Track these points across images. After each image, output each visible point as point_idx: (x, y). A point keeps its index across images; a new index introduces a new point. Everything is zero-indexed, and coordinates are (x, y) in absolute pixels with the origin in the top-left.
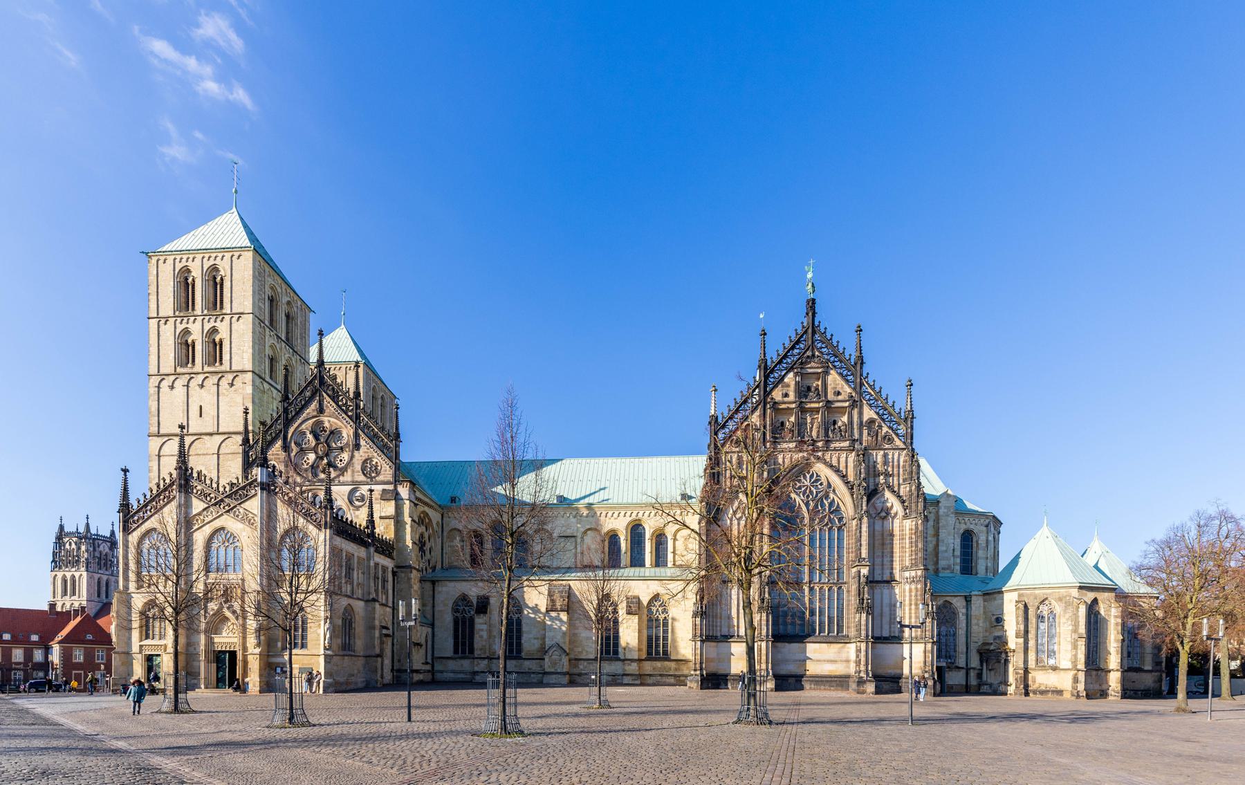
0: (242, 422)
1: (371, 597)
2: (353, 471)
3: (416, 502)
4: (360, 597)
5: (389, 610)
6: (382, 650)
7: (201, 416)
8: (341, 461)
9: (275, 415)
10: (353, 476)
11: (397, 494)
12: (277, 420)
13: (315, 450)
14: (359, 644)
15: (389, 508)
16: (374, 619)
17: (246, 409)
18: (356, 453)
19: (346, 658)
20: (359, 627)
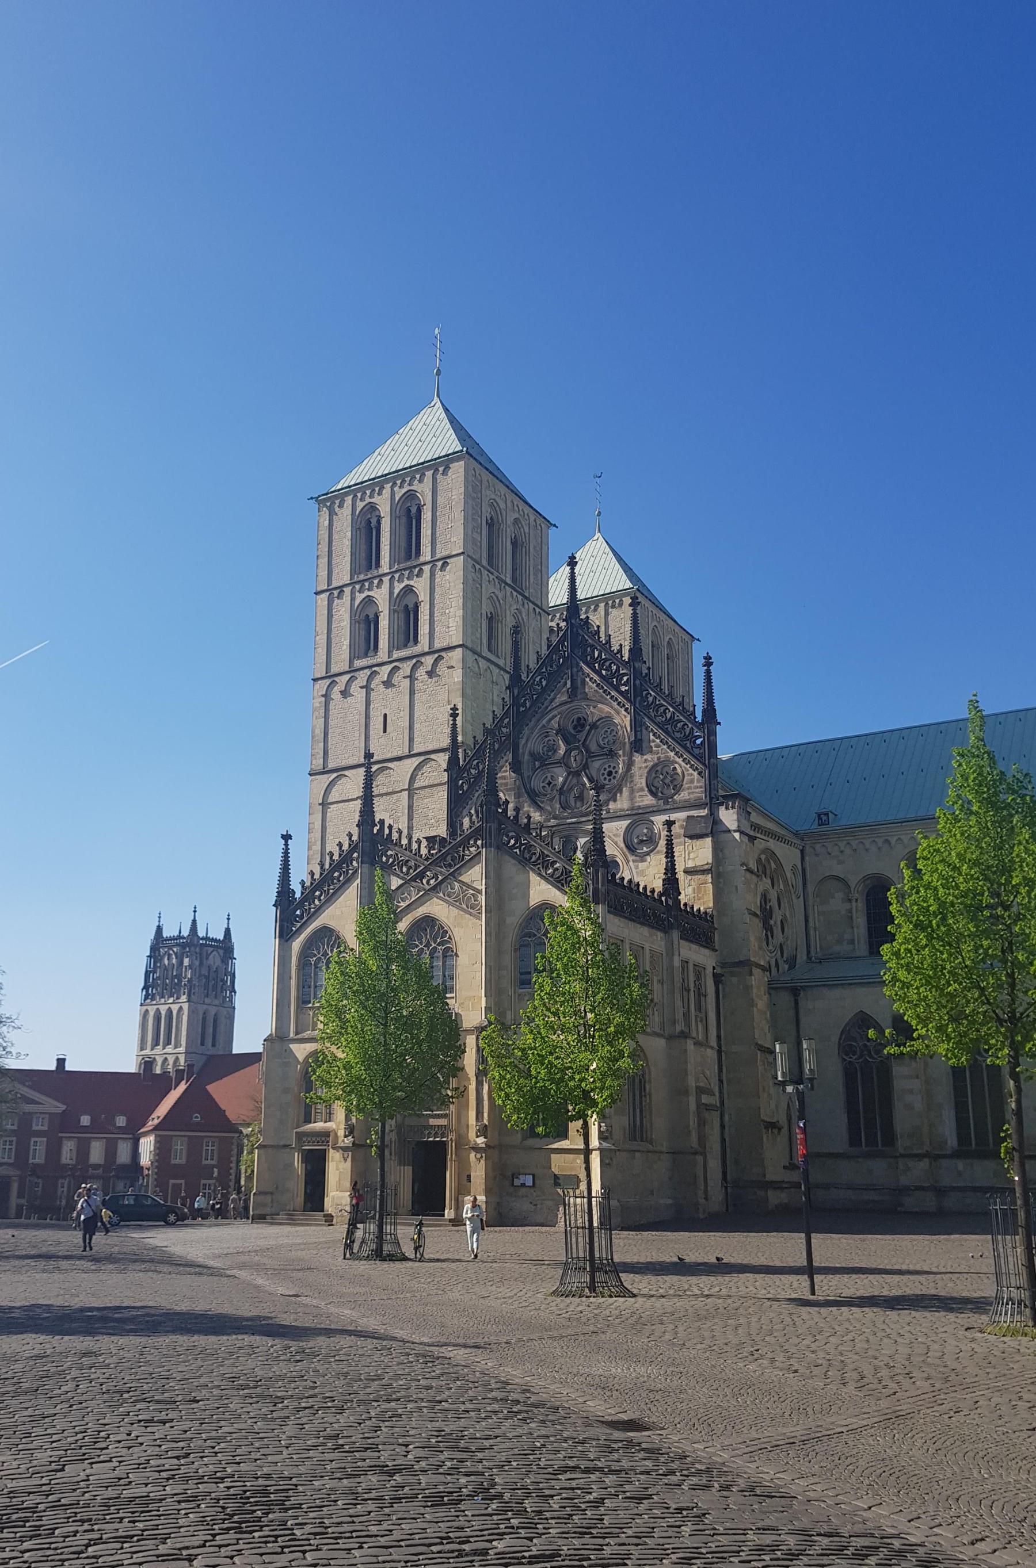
0: (448, 730)
1: (678, 1028)
2: (632, 791)
3: (752, 833)
4: (657, 1030)
5: (711, 1054)
6: (702, 1139)
7: (385, 731)
8: (610, 773)
9: (499, 713)
10: (632, 798)
11: (716, 822)
12: (502, 719)
13: (564, 762)
14: (659, 1125)
15: (702, 853)
16: (686, 1071)
17: (455, 709)
18: (637, 758)
19: (637, 1154)
20: (658, 1091)
